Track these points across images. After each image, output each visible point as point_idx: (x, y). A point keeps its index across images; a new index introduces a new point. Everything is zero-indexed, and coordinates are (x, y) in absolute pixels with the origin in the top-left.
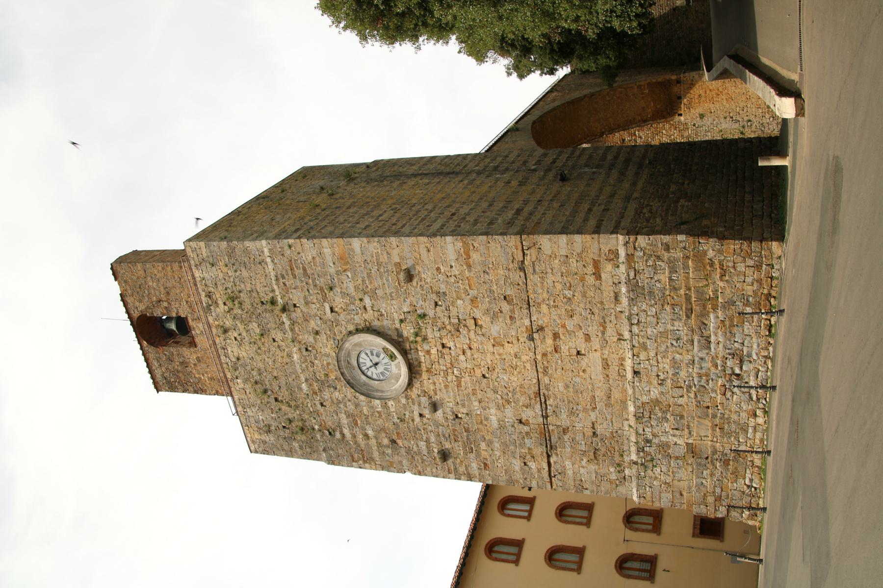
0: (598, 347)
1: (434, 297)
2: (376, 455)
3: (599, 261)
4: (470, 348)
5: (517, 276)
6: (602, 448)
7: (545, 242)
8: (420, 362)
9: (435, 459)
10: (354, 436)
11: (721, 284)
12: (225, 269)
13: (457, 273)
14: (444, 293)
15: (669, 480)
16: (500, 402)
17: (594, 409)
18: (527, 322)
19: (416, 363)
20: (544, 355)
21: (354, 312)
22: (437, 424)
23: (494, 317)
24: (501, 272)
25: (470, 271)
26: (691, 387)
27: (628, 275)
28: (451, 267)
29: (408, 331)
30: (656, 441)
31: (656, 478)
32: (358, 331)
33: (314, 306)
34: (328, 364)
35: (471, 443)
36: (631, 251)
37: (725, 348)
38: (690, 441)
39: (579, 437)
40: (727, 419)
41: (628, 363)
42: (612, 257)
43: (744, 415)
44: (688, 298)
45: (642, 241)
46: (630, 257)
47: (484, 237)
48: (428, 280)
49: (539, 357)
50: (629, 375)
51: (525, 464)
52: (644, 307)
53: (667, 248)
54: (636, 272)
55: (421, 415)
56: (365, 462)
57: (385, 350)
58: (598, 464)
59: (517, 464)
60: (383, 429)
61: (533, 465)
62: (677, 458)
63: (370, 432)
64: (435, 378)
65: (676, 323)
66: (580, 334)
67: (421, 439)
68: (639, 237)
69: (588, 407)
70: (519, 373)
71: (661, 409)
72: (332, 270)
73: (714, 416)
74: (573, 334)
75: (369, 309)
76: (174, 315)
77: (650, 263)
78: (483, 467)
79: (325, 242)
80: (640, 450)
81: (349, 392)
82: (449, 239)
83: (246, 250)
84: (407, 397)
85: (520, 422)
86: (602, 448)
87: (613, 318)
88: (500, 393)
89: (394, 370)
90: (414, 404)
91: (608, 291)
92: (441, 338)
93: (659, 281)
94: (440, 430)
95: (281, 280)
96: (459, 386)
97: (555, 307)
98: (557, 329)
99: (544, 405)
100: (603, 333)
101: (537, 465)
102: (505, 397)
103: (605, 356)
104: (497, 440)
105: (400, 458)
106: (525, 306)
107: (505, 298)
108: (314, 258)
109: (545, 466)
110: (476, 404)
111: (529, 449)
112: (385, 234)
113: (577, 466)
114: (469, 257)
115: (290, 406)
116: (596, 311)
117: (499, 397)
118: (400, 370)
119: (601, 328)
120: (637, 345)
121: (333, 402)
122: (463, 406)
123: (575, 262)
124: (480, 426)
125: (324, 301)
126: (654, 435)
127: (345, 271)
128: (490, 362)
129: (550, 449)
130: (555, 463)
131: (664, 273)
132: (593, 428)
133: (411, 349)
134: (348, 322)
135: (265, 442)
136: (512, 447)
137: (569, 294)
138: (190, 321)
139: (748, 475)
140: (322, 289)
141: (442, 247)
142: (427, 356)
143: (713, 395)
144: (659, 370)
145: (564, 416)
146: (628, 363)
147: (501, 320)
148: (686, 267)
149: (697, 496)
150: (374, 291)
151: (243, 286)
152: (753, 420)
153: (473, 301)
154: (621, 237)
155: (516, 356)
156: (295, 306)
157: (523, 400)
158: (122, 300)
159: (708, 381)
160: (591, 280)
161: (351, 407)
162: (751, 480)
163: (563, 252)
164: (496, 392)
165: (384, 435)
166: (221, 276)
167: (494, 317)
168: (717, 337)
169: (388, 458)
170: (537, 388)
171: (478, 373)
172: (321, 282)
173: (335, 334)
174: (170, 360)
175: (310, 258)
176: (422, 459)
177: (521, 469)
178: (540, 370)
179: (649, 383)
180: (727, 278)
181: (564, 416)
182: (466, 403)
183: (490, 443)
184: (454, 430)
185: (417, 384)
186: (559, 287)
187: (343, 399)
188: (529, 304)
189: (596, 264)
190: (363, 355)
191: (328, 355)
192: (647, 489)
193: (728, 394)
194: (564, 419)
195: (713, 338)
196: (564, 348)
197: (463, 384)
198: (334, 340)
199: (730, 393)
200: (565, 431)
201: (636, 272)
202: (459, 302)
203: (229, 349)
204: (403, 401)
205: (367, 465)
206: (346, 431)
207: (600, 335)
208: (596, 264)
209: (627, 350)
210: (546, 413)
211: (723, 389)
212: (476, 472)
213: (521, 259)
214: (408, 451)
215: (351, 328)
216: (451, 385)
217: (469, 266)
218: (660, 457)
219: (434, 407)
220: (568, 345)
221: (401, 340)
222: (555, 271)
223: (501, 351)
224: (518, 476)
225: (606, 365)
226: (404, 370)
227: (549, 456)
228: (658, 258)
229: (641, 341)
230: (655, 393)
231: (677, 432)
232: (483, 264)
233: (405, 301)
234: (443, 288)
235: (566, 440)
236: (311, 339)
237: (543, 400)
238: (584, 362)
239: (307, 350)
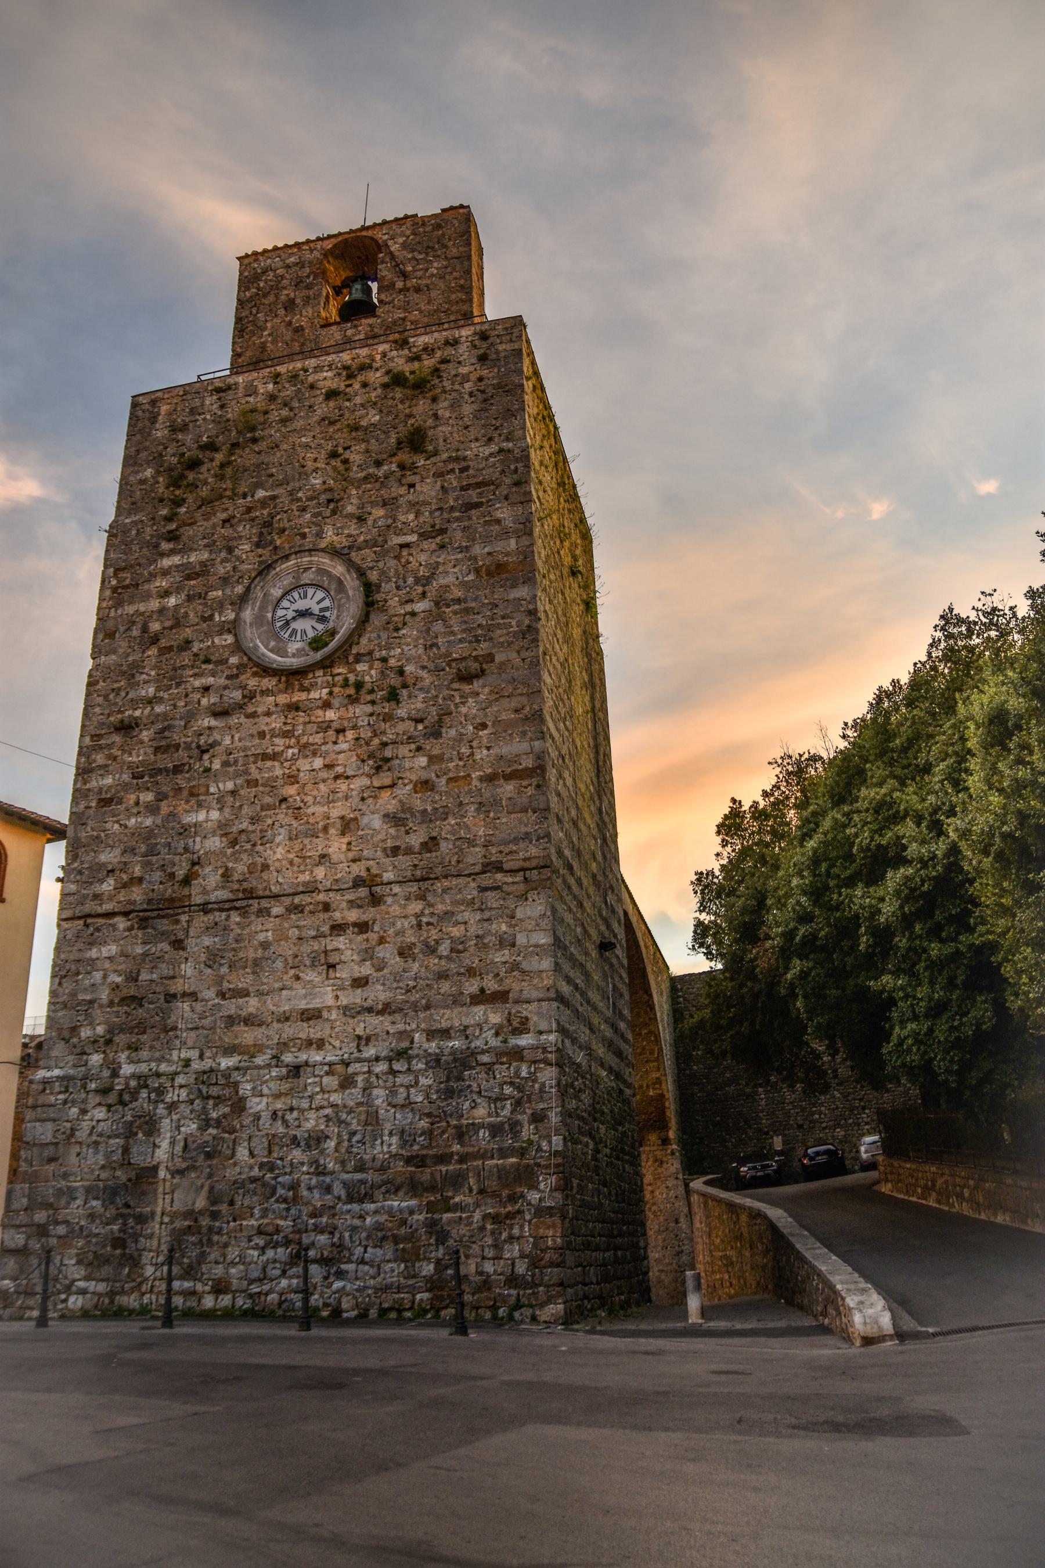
0: (344, 1001)
2: (130, 609)
3: (506, 1001)
4: (336, 778)
5: (475, 856)
8: (309, 691)
9: (120, 712)
10: (165, 573)
11: (477, 1216)
12: (473, 377)
13: (478, 757)
14: (437, 734)
15: (82, 1135)
16: (234, 829)
17: (222, 995)
18: (388, 876)
19: (306, 683)
21: (401, 582)
22: (189, 717)
23: (394, 819)
25: (481, 779)
26: (271, 1170)
27: (483, 1052)
30: (161, 1110)
31: (84, 1112)
33: (411, 517)
34: (304, 536)
35: (151, 776)
37: (354, 1229)
38: (162, 1173)
39: (165, 969)
40: (209, 1240)
41: (317, 1057)
42: (515, 1024)
43: (219, 1271)
44: (443, 1158)
46: (517, 1054)
48: (463, 710)
49: (322, 897)
51: (112, 871)
52: (423, 1081)
53: (538, 1118)
54: (489, 1068)
55: (206, 689)
56: (114, 590)
57: (333, 633)
58: (111, 1003)
59: (109, 857)
61: (108, 886)
62: (126, 1150)
63: (172, 601)
65: (395, 1140)
66: (367, 969)
67: (158, 689)
69: (226, 985)
70: (291, 863)
71: (225, 1116)
72: (477, 550)
73: (215, 1216)
75: (408, 608)
77: (508, 1090)
78: (103, 796)
80: (142, 1080)
84: (242, 667)
87: (401, 1027)
88: (251, 828)
90: (228, 678)
92: (355, 727)
93: (474, 1106)
94: (177, 723)
95: (457, 467)
96: (265, 757)
97: (419, 926)
98: (376, 928)
99: (226, 906)
100: (370, 1010)
102: (243, 837)
103: (325, 1014)
104: (159, 821)
105: (121, 651)
106: (418, 873)
107: (433, 838)
108: (498, 522)
109: (108, 907)
110: (230, 785)
111: (140, 880)
113: (107, 965)
114: (508, 777)
115: (222, 466)
116: (415, 996)
117: (244, 826)
118: (294, 656)
119: (380, 1007)
120: (351, 1070)
121: (231, 539)
122: (226, 764)
124: (185, 793)
125: (420, 535)
126: (172, 1107)
127: (477, 571)
128: (310, 811)
130: (113, 926)
131: (490, 1115)
132: (184, 994)
133: (334, 676)
134: (383, 573)
135: (154, 419)
136: (143, 848)
137: (444, 949)
138: (370, 321)
139: (91, 1285)
140: (442, 531)
141: (524, 733)
142: (320, 703)
143: (256, 1211)
144: (302, 1111)
145: (207, 941)
146: (317, 1057)
147: (392, 831)
148: (503, 1153)
150: (441, 617)
151: (446, 404)
152: (208, 1288)
153: (425, 785)
155: (323, 856)
156: (412, 486)
157: (240, 868)
158: (406, 217)
159: (285, 1201)
160: (471, 987)
162: (83, 1292)
163: (521, 939)
164: (254, 820)
165: (168, 624)
166: (463, 370)
167: (394, 819)
168: (373, 1213)
169: (122, 629)
170: (261, 893)
171: (291, 790)
173: (359, 549)
176: (119, 689)
177: (101, 866)
178: (297, 900)
179: (277, 1096)
180: (489, 1227)
181: (207, 941)
182: (231, 769)
183: (152, 809)
184: (177, 747)
186: (457, 932)
187: (238, 558)
188: (424, 879)
189: (500, 997)
190: (320, 594)
191: (319, 535)
192: (61, 1097)
193: (260, 1241)
194: (200, 942)
196: (340, 942)
197: (269, 764)
198: (350, 547)
199: (262, 1243)
200: (178, 945)
201: (489, 1068)
202: (423, 761)
203: (330, 374)
204: (234, 660)
205: (108, 593)
206: (176, 560)
207: (366, 1005)
208: (500, 997)
210: (212, 910)
211: (270, 1229)
212: (93, 784)
213: (506, 867)
214: (137, 667)
216: (266, 742)
217: (490, 779)
218: (129, 1118)
221: (351, 659)
222: (486, 924)
223: (332, 831)
225: (310, 1016)
226: (294, 662)
227: (126, 914)
228: (518, 1103)
229: (360, 1079)
230: (257, 1105)
231: (178, 1149)
232: (496, 802)
233: (424, 668)
235: (160, 946)
237: (238, 904)
239: (330, 501)
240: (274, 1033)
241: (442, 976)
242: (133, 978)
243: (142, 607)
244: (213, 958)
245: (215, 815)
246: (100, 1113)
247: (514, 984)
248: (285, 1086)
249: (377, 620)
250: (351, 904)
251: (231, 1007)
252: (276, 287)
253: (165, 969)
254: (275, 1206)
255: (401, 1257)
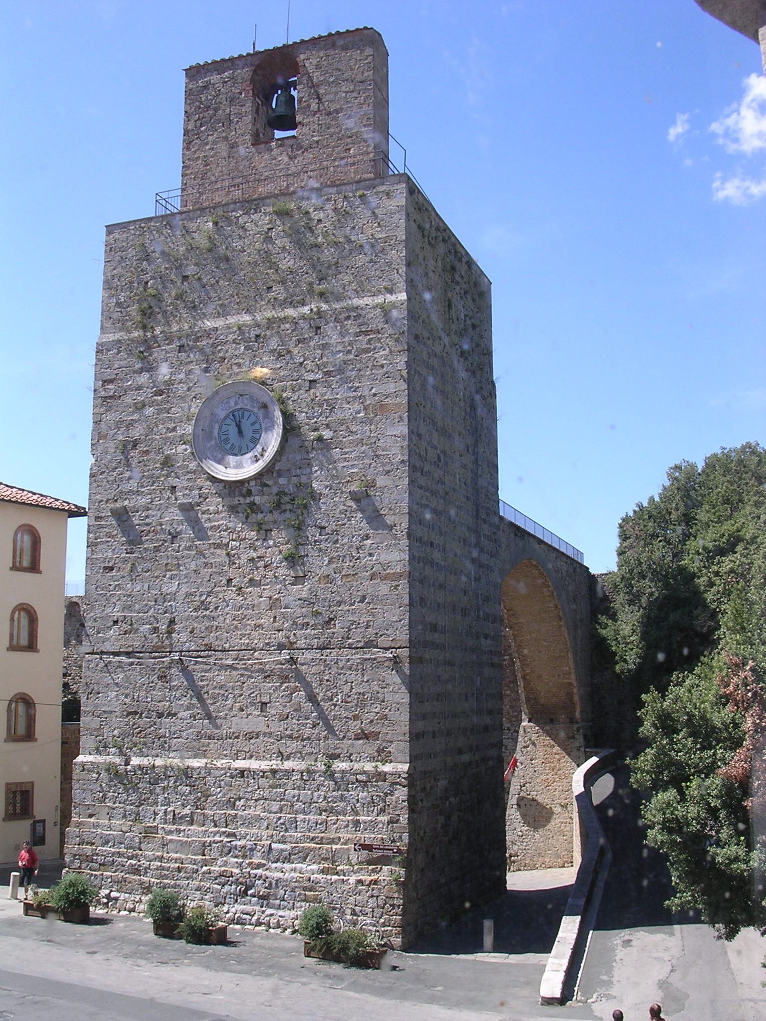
28: (371, 555)
36: (390, 779)
45: (401, 793)
46: (382, 776)
47: (407, 601)
68: (406, 789)
74: (287, 699)
85: (172, 622)
100: (290, 737)
112: (413, 469)
123: (376, 710)
154: (406, 767)
195: (287, 866)
209: (271, 763)
221: (275, 474)
249: (294, 442)
254: (232, 859)
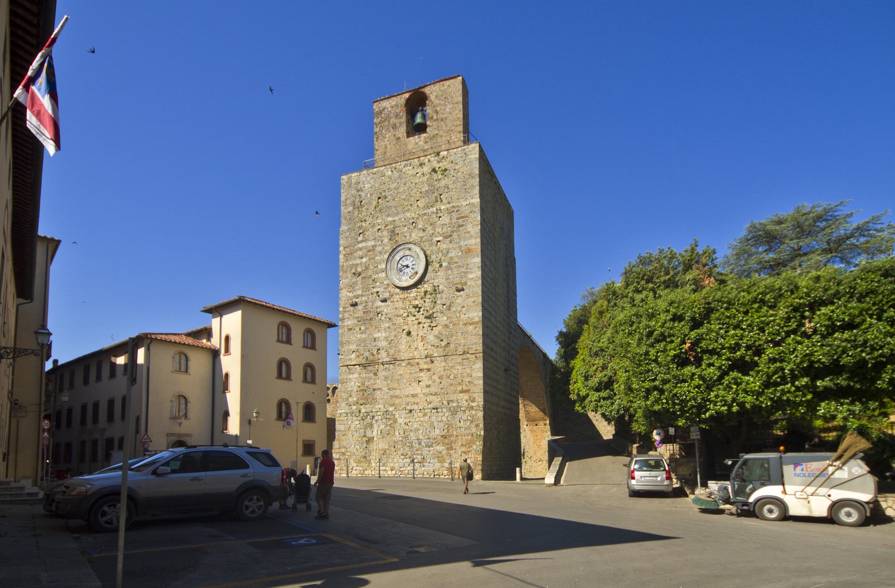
1: (448, 304)
5: (460, 350)
6: (367, 394)
7: (479, 365)
10: (361, 249)
14: (450, 310)
18: (435, 355)
20: (418, 364)
22: (373, 302)
23: (436, 337)
24: (463, 341)
29: (426, 287)
32: (426, 257)
39: (372, 382)
41: (416, 407)
43: (392, 465)
45: (480, 414)
46: (472, 408)
50: (409, 408)
53: (477, 426)
54: (464, 411)
57: (416, 273)
59: (353, 347)
60: (367, 269)
61: (353, 356)
63: (364, 260)
64: (400, 302)
66: (430, 383)
72: (462, 243)
76: (428, 123)
79: (479, 240)
81: (389, 249)
82: (481, 314)
83: (473, 187)
86: (367, 394)
89: (404, 278)
91: (453, 397)
99: (389, 363)
101: (353, 358)
109: (354, 363)
114: (471, 324)
126: (377, 421)
129: (364, 366)
137: (452, 377)
138: (425, 135)
140: (451, 236)
146: (416, 407)
149: (344, 443)
153: (446, 326)
157: (392, 352)
160: (459, 388)
161: (379, 249)
163: (474, 375)
164: (395, 336)
171: (405, 327)
172: (455, 235)
174: (397, 116)
175: (469, 230)
181: (384, 373)
185: (398, 290)
186: (455, 372)
189: (467, 391)
190: (412, 259)
191: (410, 236)
194: (382, 374)
196: (422, 374)
200: (375, 374)
201: (464, 411)
202: (445, 318)
204: (386, 282)
208: (467, 391)
214: (355, 283)
215: (428, 253)
217: (465, 324)
219: (384, 301)
220: (424, 376)
224: (346, 348)
225: (414, 396)
226: (405, 284)
230: (400, 421)
232: (467, 332)
234: (453, 309)
236: (420, 226)
238: (415, 384)
240: (405, 400)
241: (451, 385)
242: (363, 384)
243: (355, 262)
244: (386, 378)
245: (384, 334)
246: (357, 422)
247: (472, 389)
248: (408, 415)
250: (425, 363)
251: (392, 393)
252: (388, 118)
253: (372, 382)
255: (439, 462)
